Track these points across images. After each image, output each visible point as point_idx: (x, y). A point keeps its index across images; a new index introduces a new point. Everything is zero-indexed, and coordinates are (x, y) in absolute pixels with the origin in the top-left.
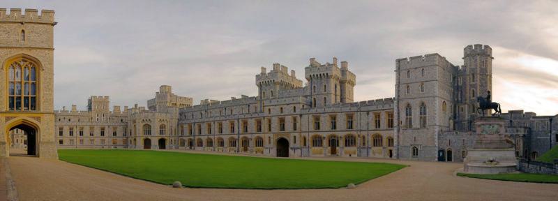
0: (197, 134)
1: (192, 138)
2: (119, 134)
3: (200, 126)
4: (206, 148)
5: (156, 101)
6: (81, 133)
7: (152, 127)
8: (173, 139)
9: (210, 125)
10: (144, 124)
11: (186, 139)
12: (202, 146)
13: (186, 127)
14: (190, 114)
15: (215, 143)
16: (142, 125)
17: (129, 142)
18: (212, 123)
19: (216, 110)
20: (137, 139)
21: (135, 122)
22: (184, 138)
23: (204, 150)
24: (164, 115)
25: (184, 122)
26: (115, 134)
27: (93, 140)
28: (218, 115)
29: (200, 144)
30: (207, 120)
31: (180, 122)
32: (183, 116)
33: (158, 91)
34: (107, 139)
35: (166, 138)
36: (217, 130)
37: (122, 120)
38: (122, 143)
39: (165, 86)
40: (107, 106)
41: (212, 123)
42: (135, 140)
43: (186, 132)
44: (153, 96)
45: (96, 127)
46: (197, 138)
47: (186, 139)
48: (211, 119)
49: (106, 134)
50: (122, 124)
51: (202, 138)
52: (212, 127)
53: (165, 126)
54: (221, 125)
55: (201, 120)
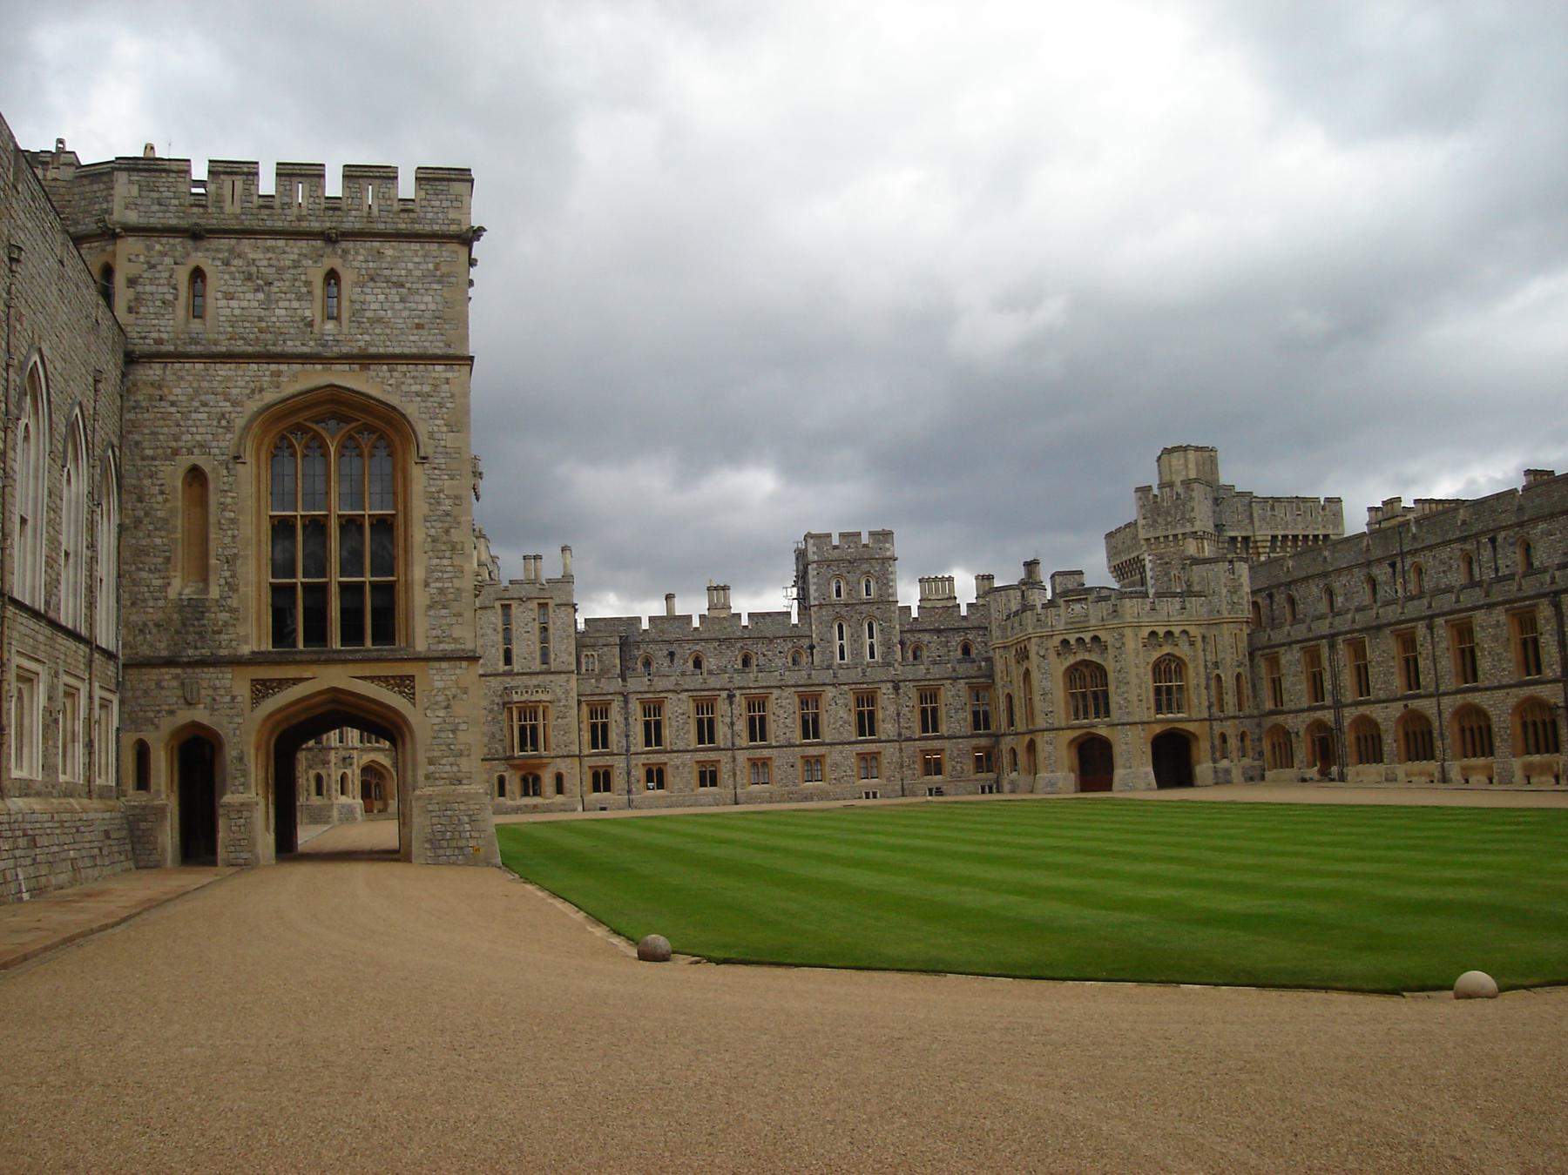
0: (1349, 695)
1: (1328, 716)
2: (955, 717)
3: (1358, 649)
4: (1401, 770)
5: (1142, 534)
6: (758, 729)
7: (1111, 677)
8: (1230, 729)
9: (1408, 642)
10: (1071, 660)
11: (1298, 724)
12: (1378, 759)
13: (1291, 659)
14: (1315, 589)
15: (1447, 737)
16: (1059, 666)
17: (1006, 759)
18: (1421, 629)
19: (1444, 553)
20: (1041, 741)
21: (1023, 655)
22: (1290, 722)
23: (1391, 779)
24: (1170, 607)
25: (1278, 636)
26: (929, 720)
27: (819, 760)
28: (1457, 578)
29: (1371, 750)
30: (1391, 614)
31: (1263, 638)
32: (1280, 598)
33: (1154, 482)
34: (889, 752)
35: (1191, 727)
36: (1447, 663)
37: (966, 650)
38: (969, 766)
39: (1185, 449)
40: (886, 582)
41: (1421, 629)
42: (1031, 747)
43: (1297, 688)
44: (1129, 511)
45: (830, 692)
46: (1349, 714)
47: (1298, 724)
48: (1413, 609)
49: (886, 728)
50: (962, 669)
51: (1378, 713)
52: (1424, 651)
53: (1181, 664)
54: (1464, 632)
55: (1362, 620)
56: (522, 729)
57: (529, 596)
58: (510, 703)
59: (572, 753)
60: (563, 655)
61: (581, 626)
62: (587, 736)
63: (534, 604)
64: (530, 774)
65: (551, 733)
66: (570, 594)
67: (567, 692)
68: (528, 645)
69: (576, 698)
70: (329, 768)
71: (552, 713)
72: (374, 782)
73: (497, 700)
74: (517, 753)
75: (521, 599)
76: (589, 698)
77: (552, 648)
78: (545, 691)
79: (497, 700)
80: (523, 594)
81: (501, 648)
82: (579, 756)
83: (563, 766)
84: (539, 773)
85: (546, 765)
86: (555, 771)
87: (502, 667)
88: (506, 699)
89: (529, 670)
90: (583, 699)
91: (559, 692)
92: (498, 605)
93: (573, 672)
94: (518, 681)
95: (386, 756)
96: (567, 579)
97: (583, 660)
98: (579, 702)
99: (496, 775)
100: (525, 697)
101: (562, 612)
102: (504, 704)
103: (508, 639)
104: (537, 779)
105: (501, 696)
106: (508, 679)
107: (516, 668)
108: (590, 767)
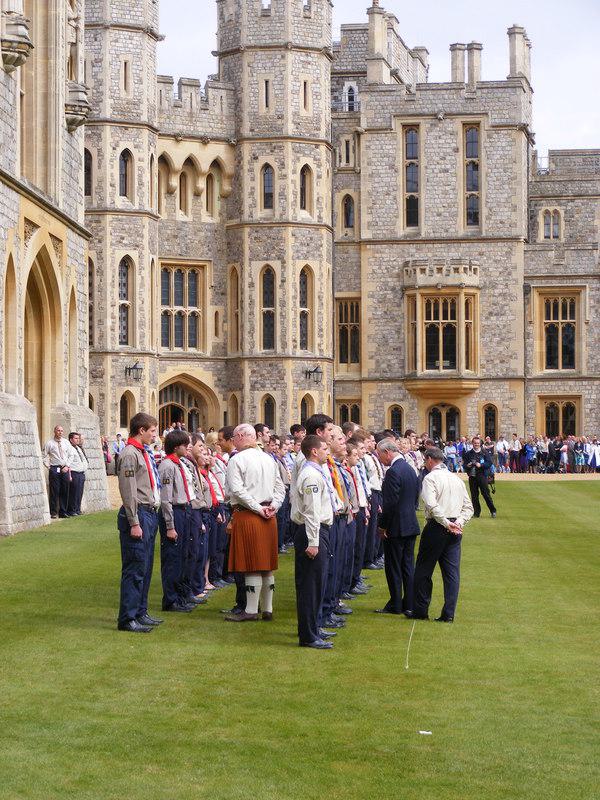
56: (431, 331)
57: (448, 110)
58: (412, 287)
59: (511, 374)
60: (506, 207)
61: (544, 163)
62: (539, 347)
63: (456, 125)
64: (443, 406)
65: (478, 339)
66: (516, 106)
67: (507, 272)
68: (446, 193)
69: (521, 282)
70: (103, 384)
71: (480, 307)
72: (187, 410)
73: (393, 281)
74: (422, 370)
75: (435, 115)
76: (544, 283)
77: (483, 198)
78: (471, 268)
79: (393, 281)
80: (440, 107)
81: (401, 197)
82: (523, 379)
83: (497, 395)
84: (458, 404)
85: (469, 392)
86: (483, 402)
87: (401, 229)
88: (408, 282)
89: (444, 235)
90: (534, 284)
91: (494, 271)
92: (397, 125)
93: (516, 239)
94: (426, 253)
95: (206, 369)
96: (517, 82)
97: (541, 219)
98: (527, 290)
99: (388, 405)
100: (436, 279)
101: (502, 139)
102: (404, 289)
103: (412, 183)
104: (454, 415)
105: (398, 276)
106: (412, 249)
107: (425, 228)
108: (541, 398)
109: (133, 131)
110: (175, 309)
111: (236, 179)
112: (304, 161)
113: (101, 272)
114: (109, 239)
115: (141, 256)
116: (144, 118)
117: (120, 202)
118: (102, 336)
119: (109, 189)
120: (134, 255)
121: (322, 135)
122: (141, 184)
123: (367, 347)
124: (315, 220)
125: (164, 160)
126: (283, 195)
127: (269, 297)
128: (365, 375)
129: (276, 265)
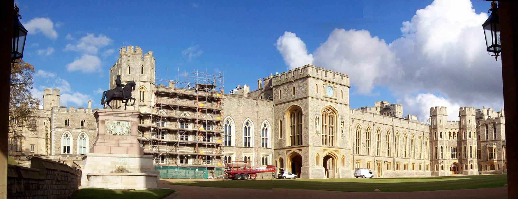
99: (485, 165)
109: (442, 129)
110: (453, 153)
111: (461, 134)
112: (470, 131)
113: (438, 149)
114: (439, 144)
115: (444, 146)
116: (444, 127)
117: (440, 139)
118: (438, 158)
119: (438, 137)
120: (443, 146)
121: (473, 127)
122: (443, 136)
123: (482, 157)
124: (472, 139)
125: (450, 133)
126: (467, 136)
127: (465, 151)
128: (482, 161)
129: (466, 146)
